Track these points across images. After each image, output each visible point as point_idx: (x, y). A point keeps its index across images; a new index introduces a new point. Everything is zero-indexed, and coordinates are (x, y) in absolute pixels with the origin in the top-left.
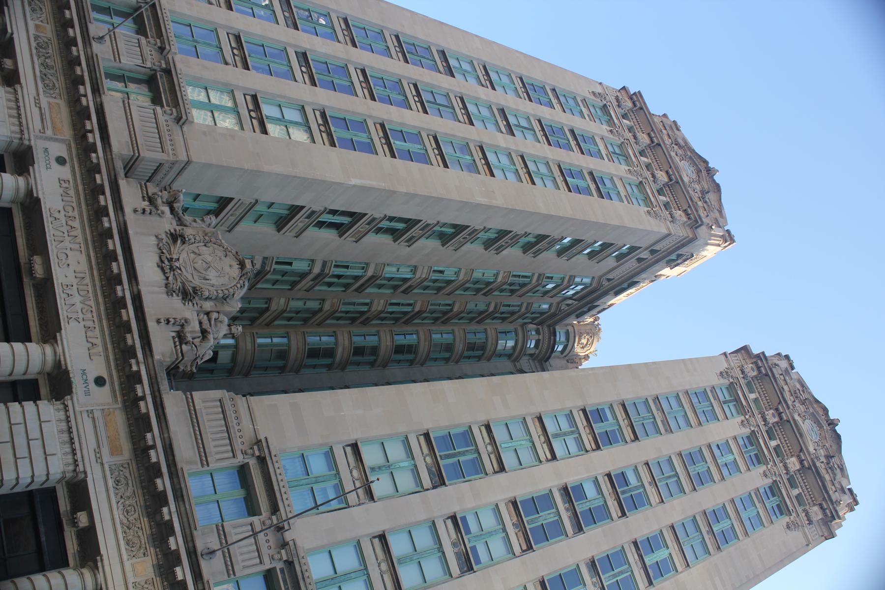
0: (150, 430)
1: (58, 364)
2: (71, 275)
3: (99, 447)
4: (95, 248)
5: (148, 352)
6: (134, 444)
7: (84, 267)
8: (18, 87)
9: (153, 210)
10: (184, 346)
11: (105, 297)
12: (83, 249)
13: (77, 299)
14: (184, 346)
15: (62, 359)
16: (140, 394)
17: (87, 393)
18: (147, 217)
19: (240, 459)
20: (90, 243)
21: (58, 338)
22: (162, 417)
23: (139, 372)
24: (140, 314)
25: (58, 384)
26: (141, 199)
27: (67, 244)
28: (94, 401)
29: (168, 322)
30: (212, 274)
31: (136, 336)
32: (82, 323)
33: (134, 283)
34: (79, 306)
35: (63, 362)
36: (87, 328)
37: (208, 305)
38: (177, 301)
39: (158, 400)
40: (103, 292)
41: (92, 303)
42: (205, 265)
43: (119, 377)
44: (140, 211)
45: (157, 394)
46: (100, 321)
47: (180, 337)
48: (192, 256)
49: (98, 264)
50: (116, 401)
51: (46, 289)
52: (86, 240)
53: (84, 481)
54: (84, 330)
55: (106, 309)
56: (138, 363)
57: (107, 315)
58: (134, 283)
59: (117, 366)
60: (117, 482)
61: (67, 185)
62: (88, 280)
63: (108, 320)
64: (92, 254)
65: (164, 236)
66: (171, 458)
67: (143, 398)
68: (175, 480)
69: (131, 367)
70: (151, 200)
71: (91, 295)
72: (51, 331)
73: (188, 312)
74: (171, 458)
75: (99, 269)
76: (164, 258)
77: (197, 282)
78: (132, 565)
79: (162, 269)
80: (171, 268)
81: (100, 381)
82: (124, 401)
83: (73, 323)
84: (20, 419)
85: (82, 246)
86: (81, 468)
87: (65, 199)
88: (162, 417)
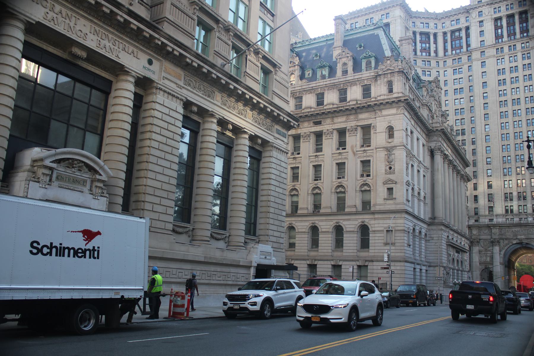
0: (186, 57)
3: (176, 84)
4: (78, 8)
5: (158, 31)
6: (180, 67)
7: (88, 24)
11: (110, 26)
12: (78, 17)
13: (105, 42)
15: (138, 75)
17: (154, 73)
20: (75, 9)
21: (128, 70)
22: (186, 48)
23: (162, 43)
24: (139, 19)
27: (72, 24)
28: (159, 71)
31: (147, 30)
33: (122, 8)
34: (111, 45)
35: (140, 76)
36: (124, 50)
39: (179, 44)
40: (107, 25)
41: (110, 36)
43: (152, 51)
45: (176, 42)
46: (122, 39)
49: (89, 14)
50: (161, 60)
51: (94, 56)
52: (71, 9)
53: (187, 100)
54: (124, 52)
55: (117, 30)
56: (159, 40)
57: (120, 32)
58: (122, 8)
59: (146, 48)
60: (189, 85)
62: (97, 29)
63: (123, 34)
64: (81, 12)
66: (201, 58)
67: (173, 49)
68: (208, 63)
69: (159, 44)
71: (106, 33)
72: (119, 70)
74: (201, 58)
75: (93, 16)
78: (216, 100)
81: (150, 62)
82: (162, 57)
84: (160, 114)
85: (74, 15)
86: (184, 99)
88: (186, 48)
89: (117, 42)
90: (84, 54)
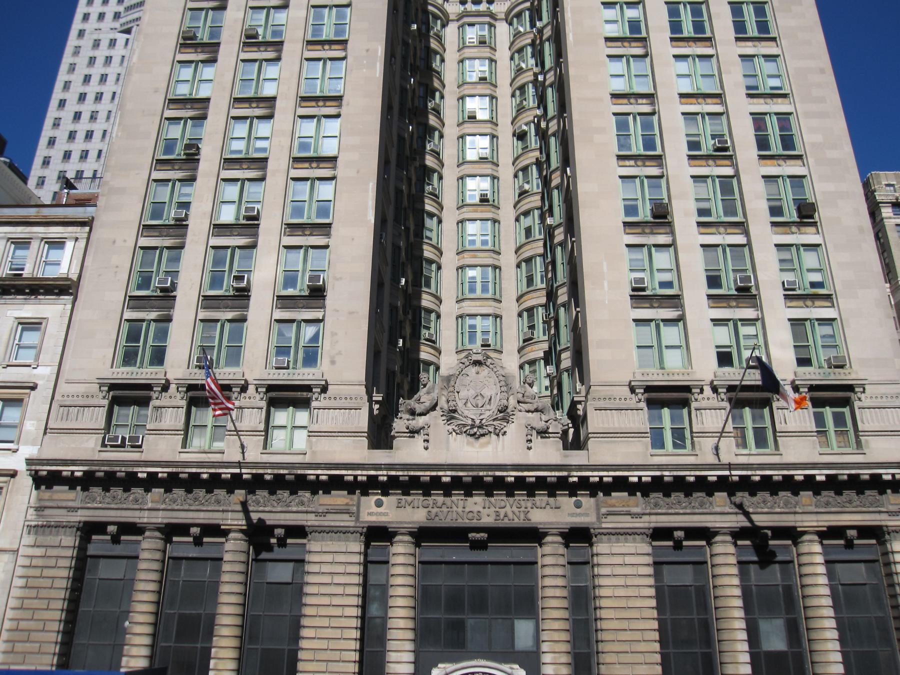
1: (562, 534)
2: (487, 511)
8: (307, 529)
9: (426, 432)
10: (550, 430)
14: (550, 430)
16: (597, 479)
17: (587, 515)
18: (431, 438)
19: (643, 405)
25: (579, 536)
26: (412, 439)
29: (531, 441)
30: (487, 393)
32: (529, 509)
37: (512, 402)
38: (511, 428)
42: (479, 397)
44: (426, 444)
47: (543, 433)
48: (469, 405)
61: (403, 502)
65: (450, 428)
70: (413, 432)
73: (521, 419)
76: (472, 432)
77: (494, 407)
79: (483, 435)
80: (480, 427)
81: (578, 505)
83: (530, 516)
87: (416, 505)
89: (522, 503)
90: (484, 535)
